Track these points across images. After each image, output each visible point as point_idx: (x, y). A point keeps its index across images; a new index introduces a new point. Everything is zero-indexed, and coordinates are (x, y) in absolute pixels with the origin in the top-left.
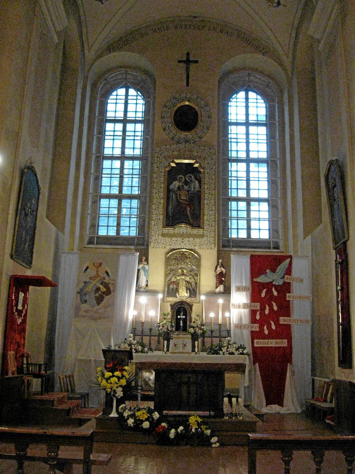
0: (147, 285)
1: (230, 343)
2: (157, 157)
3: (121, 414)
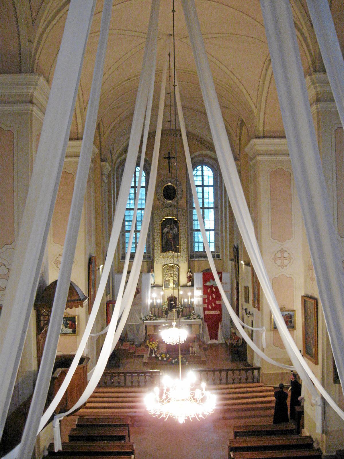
0: (154, 283)
1: (194, 314)
2: (156, 216)
3: (156, 356)
